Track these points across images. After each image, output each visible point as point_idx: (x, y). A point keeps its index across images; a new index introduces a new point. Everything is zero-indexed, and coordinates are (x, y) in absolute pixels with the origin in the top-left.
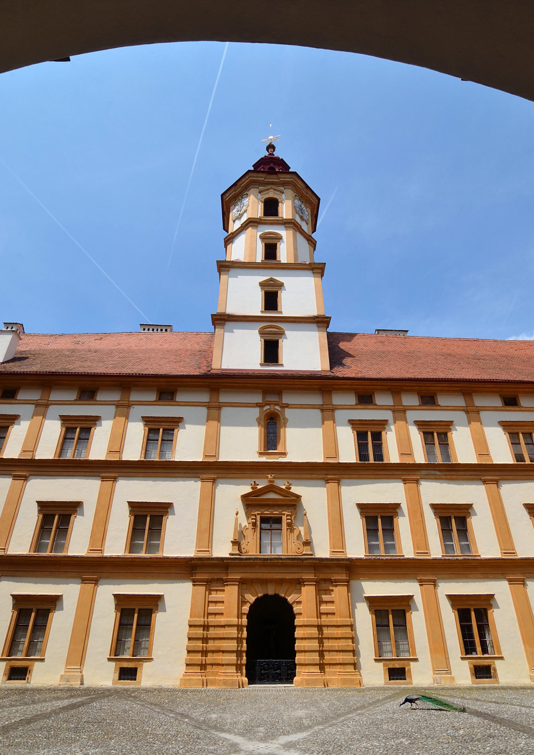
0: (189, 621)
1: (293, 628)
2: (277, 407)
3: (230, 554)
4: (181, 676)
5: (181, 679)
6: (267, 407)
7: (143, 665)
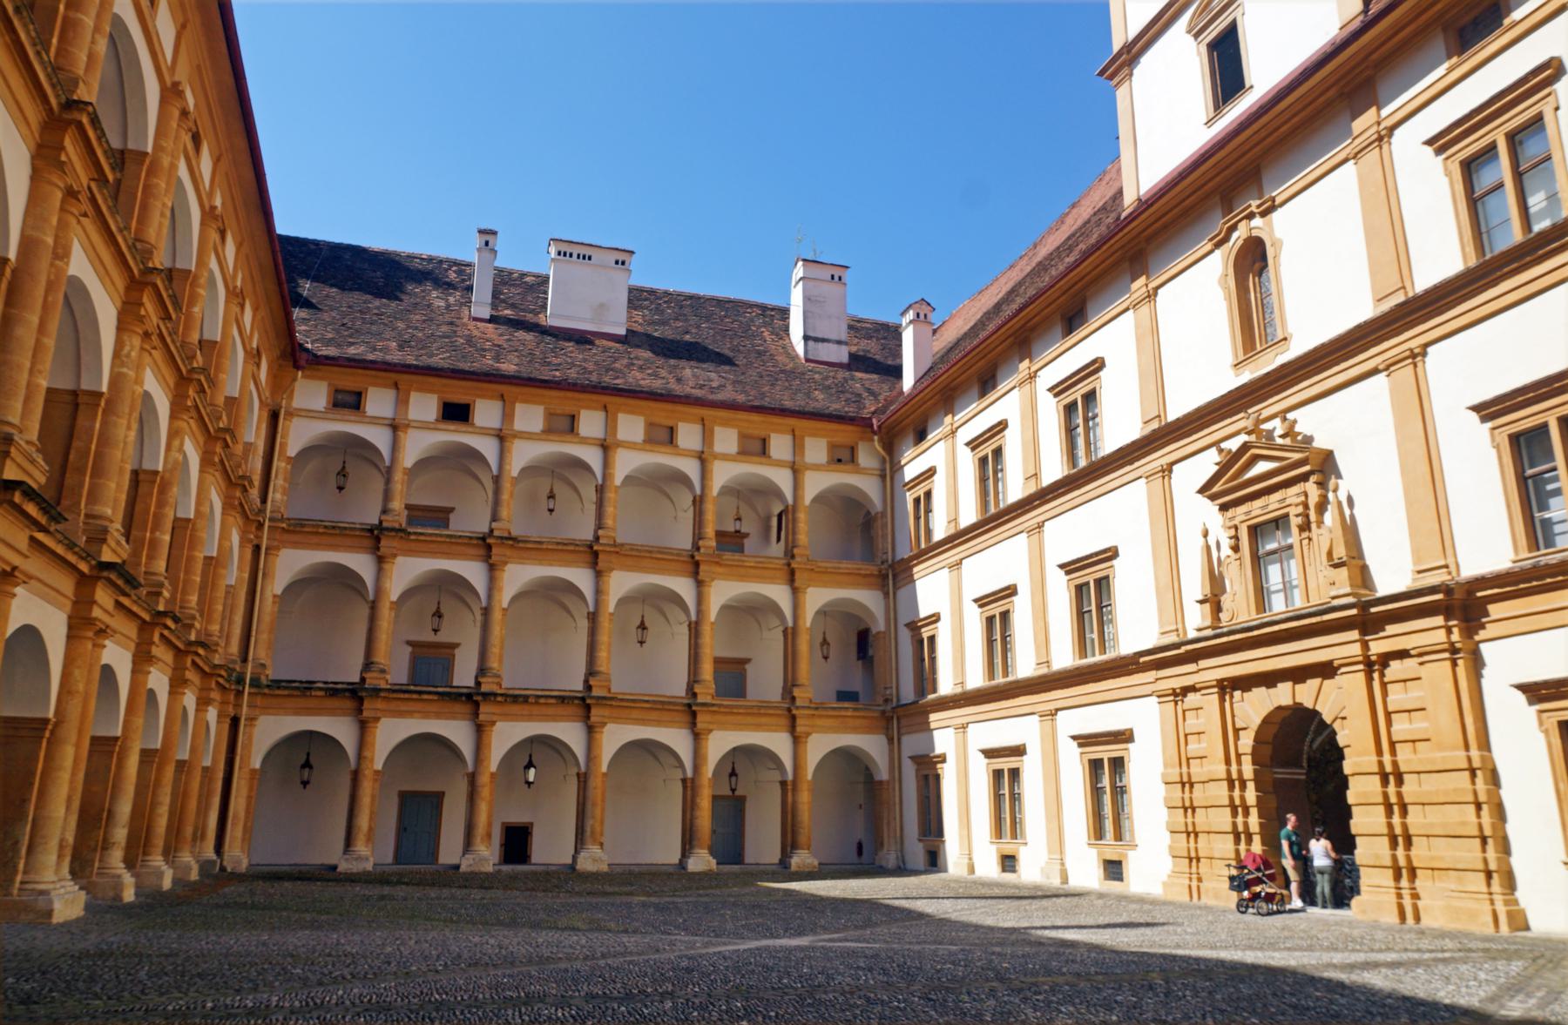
0: (1163, 775)
1: (1343, 783)
2: (1257, 222)
3: (1199, 630)
4: (1165, 878)
5: (1164, 884)
6: (1235, 235)
7: (1126, 856)
